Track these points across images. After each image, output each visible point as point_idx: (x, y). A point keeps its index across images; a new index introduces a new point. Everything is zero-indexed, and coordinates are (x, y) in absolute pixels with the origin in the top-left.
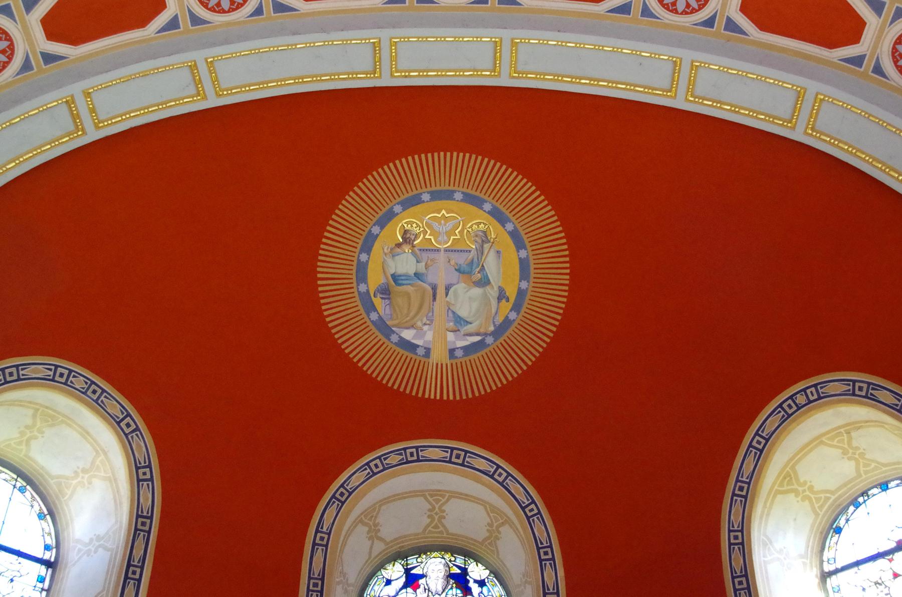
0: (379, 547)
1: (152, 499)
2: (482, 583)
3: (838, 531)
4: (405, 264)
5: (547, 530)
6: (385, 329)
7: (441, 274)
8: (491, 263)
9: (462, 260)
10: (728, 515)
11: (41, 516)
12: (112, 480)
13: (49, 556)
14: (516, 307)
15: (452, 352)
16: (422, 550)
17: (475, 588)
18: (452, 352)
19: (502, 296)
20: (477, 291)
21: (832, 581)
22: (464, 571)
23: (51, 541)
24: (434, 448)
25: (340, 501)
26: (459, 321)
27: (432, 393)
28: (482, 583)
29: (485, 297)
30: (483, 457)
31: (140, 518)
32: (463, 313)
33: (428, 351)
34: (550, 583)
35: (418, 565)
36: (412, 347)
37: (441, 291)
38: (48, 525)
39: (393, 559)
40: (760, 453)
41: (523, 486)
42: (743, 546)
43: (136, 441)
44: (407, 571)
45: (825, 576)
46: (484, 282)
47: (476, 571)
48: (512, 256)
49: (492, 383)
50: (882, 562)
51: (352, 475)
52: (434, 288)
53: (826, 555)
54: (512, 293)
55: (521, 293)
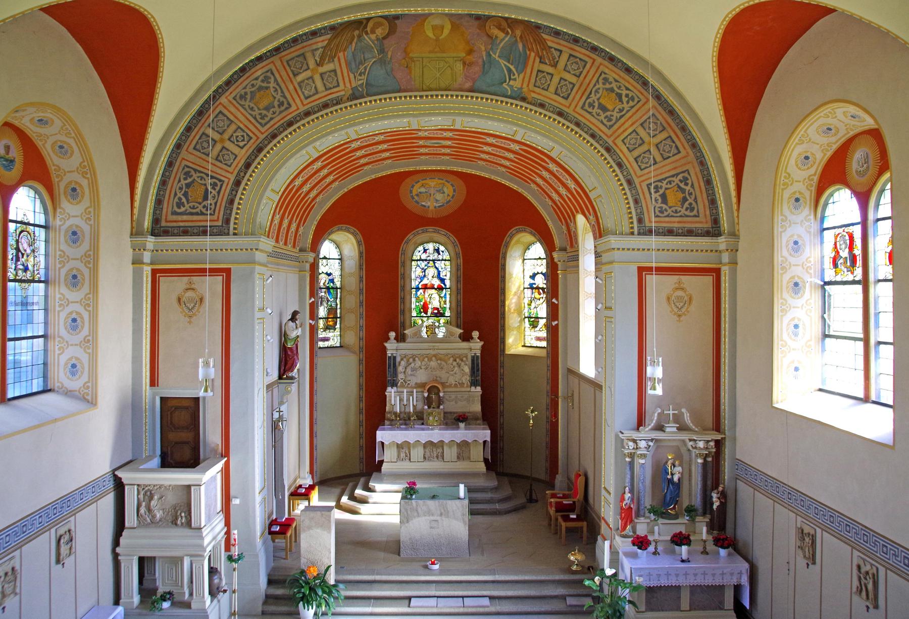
0: (416, 245)
1: (363, 248)
2: (443, 252)
3: (529, 249)
4: (423, 190)
5: (459, 249)
6: (418, 203)
7: (432, 191)
8: (445, 190)
9: (438, 189)
10: (502, 250)
11: (336, 248)
12: (353, 244)
13: (339, 257)
14: (452, 197)
15: (435, 207)
16: (428, 242)
17: (441, 253)
18: (435, 207)
19: (448, 195)
20: (442, 195)
21: (525, 261)
22: (439, 248)
23: (339, 254)
24: (430, 229)
25: (407, 243)
26: (437, 200)
27: (430, 216)
28: (443, 252)
29: (444, 197)
30: (443, 231)
31: (361, 253)
32: (438, 199)
33: (429, 207)
34: (459, 263)
35: (427, 246)
36: (425, 206)
37: (432, 195)
38: (338, 250)
39: (420, 245)
40: (511, 237)
41: (453, 238)
42: (505, 258)
43: (358, 237)
44: (424, 248)
45: (524, 259)
46: (444, 193)
47: (442, 248)
48: (451, 189)
49: (445, 214)
50: (535, 261)
51: (410, 236)
52: (430, 194)
53: (526, 254)
54: (451, 195)
55: (453, 195)
